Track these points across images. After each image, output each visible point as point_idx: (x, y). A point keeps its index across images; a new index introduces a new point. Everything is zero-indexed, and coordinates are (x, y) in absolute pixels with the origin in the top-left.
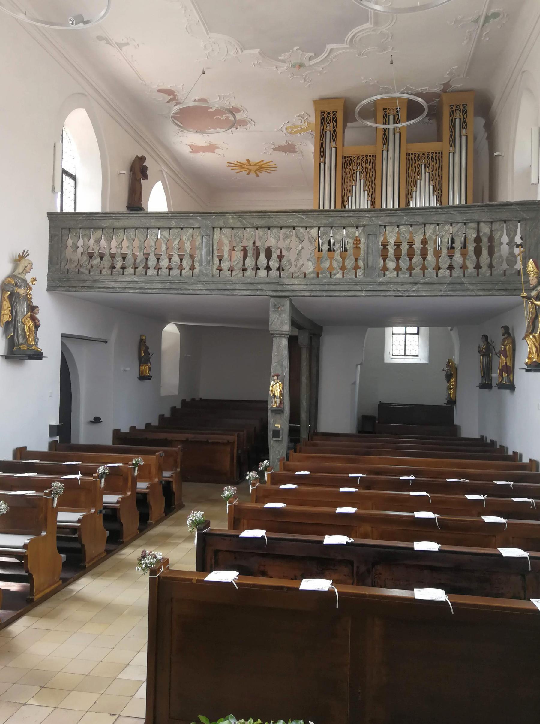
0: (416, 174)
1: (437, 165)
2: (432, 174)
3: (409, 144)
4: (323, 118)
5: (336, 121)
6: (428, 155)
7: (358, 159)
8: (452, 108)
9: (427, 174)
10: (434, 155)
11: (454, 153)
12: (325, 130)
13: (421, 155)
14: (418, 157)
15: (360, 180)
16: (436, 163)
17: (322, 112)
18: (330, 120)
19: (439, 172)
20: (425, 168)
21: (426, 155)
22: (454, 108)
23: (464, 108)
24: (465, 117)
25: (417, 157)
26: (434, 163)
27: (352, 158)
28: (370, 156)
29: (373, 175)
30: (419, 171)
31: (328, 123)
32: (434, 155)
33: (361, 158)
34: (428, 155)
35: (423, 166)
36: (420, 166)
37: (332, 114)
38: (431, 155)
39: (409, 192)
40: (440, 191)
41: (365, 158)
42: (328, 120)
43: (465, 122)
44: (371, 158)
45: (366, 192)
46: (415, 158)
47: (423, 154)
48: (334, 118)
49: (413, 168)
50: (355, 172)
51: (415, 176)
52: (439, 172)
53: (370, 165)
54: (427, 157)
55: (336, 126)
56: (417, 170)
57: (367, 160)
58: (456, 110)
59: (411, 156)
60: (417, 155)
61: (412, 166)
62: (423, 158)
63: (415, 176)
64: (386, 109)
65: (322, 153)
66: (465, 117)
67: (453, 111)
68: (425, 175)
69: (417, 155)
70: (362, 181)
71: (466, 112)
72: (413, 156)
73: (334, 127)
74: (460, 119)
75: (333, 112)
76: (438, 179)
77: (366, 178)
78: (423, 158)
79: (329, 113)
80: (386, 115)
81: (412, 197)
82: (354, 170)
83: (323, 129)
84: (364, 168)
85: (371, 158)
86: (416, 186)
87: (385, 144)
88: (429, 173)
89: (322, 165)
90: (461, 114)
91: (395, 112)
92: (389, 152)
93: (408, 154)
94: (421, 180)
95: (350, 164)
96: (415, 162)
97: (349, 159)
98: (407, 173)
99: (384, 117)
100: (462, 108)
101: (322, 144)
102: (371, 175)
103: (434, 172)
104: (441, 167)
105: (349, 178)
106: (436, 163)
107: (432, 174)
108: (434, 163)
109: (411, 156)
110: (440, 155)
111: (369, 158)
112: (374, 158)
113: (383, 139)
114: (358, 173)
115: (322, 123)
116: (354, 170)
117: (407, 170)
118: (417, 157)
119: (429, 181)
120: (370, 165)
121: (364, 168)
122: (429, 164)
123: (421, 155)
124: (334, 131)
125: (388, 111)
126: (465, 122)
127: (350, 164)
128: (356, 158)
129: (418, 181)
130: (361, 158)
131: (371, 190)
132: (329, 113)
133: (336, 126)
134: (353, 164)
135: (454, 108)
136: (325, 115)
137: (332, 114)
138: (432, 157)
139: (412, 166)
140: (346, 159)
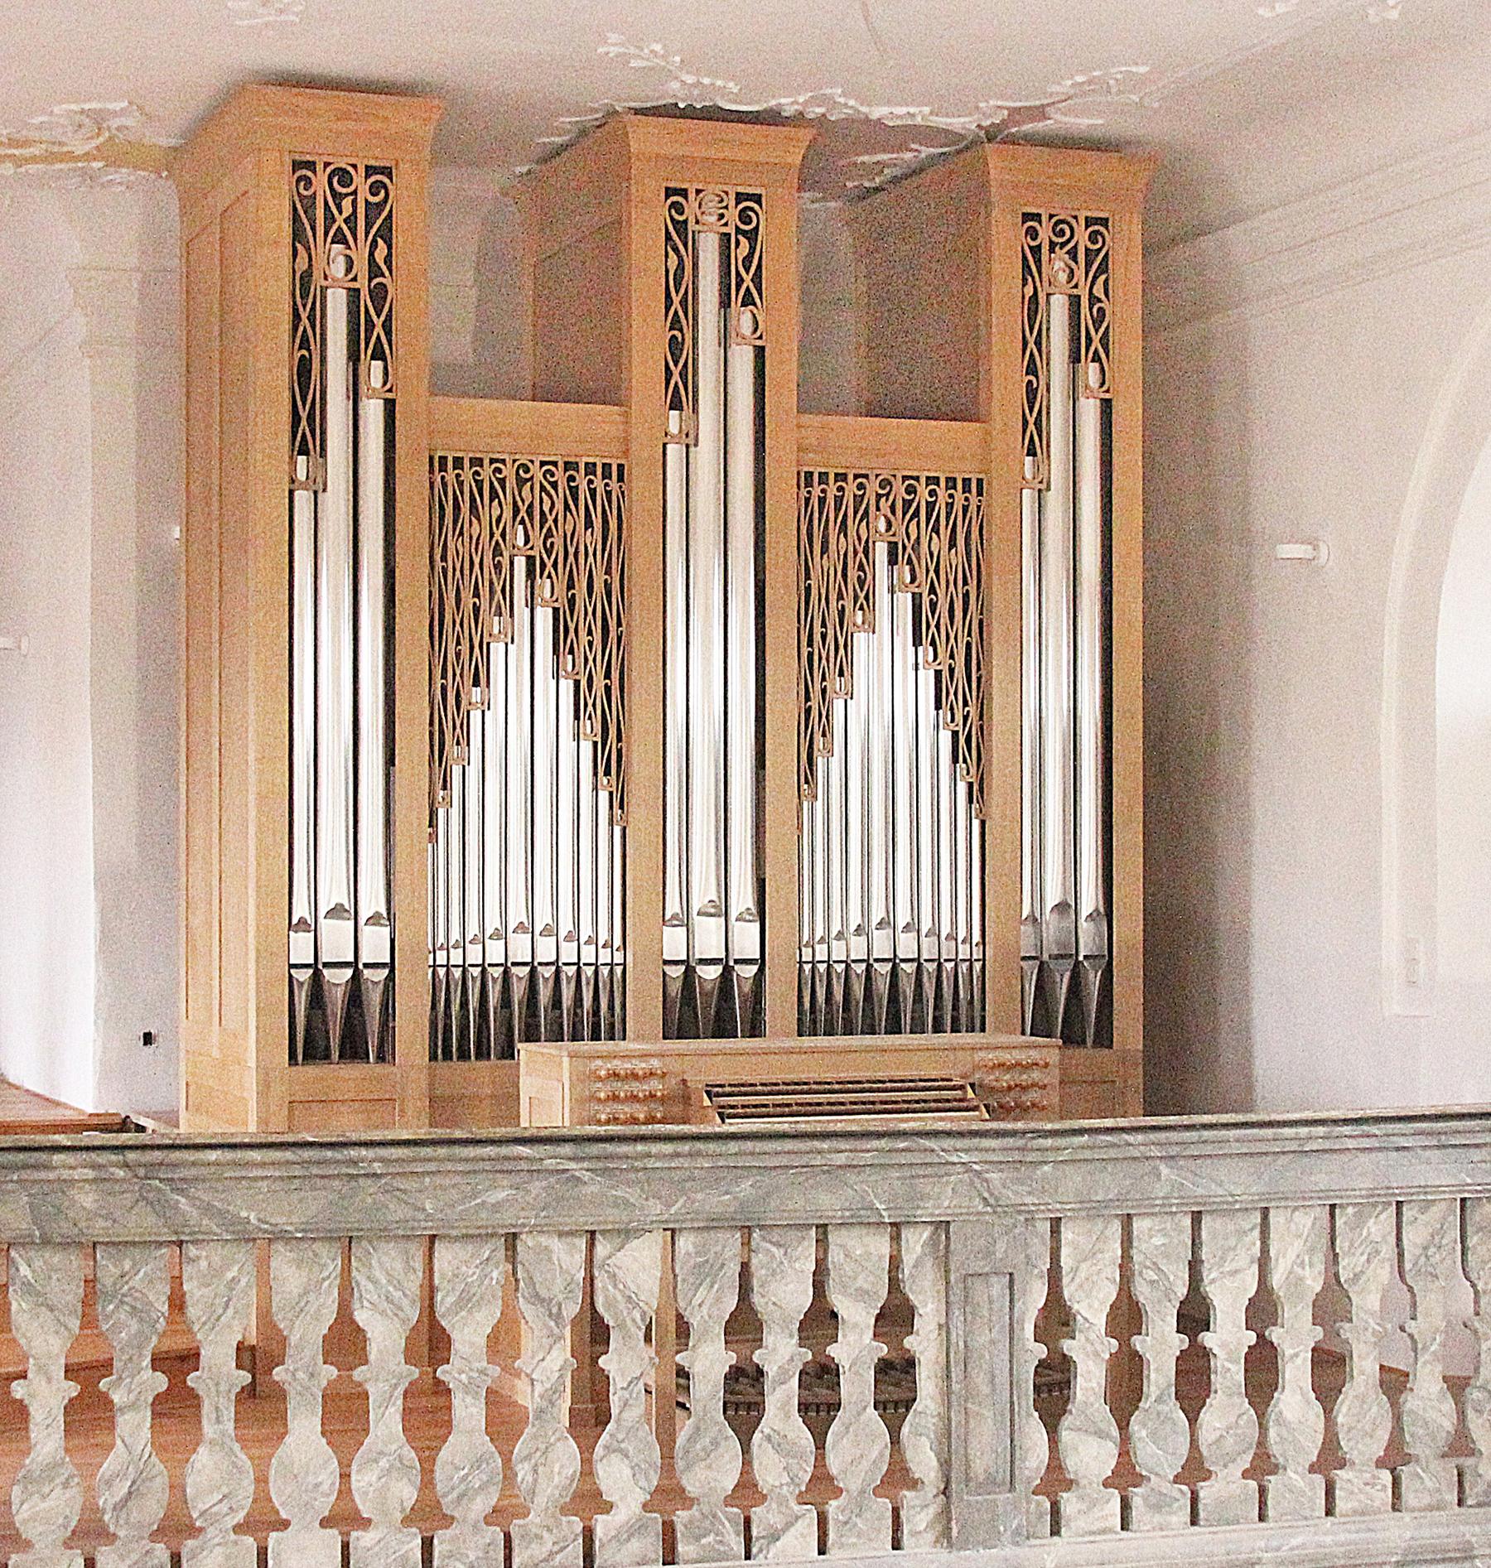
0: (848, 603)
1: (957, 558)
2: (933, 606)
4: (309, 204)
5: (386, 233)
6: (911, 490)
7: (521, 482)
8: (1033, 233)
10: (942, 493)
12: (318, 279)
13: (873, 487)
14: (858, 500)
16: (952, 544)
17: (296, 165)
18: (351, 220)
21: (899, 489)
22: (1045, 233)
23: (1093, 238)
24: (1098, 291)
25: (849, 499)
26: (940, 544)
27: (486, 472)
28: (590, 469)
31: (340, 238)
32: (942, 493)
34: (911, 490)
35: (881, 551)
37: (361, 183)
39: (814, 704)
40: (972, 710)
41: (560, 476)
42: (340, 221)
43: (1097, 323)
44: (599, 484)
46: (839, 501)
47: (885, 483)
48: (373, 210)
49: (832, 562)
52: (966, 595)
53: (589, 524)
54: (907, 504)
55: (388, 260)
56: (853, 574)
57: (574, 492)
58: (1052, 245)
59: (816, 491)
60: (851, 488)
61: (824, 550)
64: (684, 193)
66: (1098, 291)
67: (1036, 251)
70: (544, 617)
71: (1103, 268)
72: (832, 491)
73: (374, 271)
74: (1075, 301)
75: (370, 170)
77: (572, 601)
79: (344, 176)
80: (680, 227)
82: (497, 551)
83: (307, 276)
89: (302, 498)
90: (1080, 272)
91: (732, 215)
97: (467, 475)
99: (668, 237)
100: (1082, 237)
102: (598, 586)
103: (941, 592)
104: (976, 572)
105: (468, 600)
106: (952, 544)
107: (933, 606)
109: (816, 491)
110: (974, 500)
111: (582, 483)
115: (297, 235)
116: (497, 551)
118: (849, 499)
120: (589, 524)
123: (873, 487)
124: (379, 295)
125: (691, 208)
126: (1097, 323)
128: (508, 472)
132: (344, 176)
133: (388, 260)
135: (1045, 233)
136: (320, 182)
137: (361, 183)
138: (931, 506)
139: (824, 550)
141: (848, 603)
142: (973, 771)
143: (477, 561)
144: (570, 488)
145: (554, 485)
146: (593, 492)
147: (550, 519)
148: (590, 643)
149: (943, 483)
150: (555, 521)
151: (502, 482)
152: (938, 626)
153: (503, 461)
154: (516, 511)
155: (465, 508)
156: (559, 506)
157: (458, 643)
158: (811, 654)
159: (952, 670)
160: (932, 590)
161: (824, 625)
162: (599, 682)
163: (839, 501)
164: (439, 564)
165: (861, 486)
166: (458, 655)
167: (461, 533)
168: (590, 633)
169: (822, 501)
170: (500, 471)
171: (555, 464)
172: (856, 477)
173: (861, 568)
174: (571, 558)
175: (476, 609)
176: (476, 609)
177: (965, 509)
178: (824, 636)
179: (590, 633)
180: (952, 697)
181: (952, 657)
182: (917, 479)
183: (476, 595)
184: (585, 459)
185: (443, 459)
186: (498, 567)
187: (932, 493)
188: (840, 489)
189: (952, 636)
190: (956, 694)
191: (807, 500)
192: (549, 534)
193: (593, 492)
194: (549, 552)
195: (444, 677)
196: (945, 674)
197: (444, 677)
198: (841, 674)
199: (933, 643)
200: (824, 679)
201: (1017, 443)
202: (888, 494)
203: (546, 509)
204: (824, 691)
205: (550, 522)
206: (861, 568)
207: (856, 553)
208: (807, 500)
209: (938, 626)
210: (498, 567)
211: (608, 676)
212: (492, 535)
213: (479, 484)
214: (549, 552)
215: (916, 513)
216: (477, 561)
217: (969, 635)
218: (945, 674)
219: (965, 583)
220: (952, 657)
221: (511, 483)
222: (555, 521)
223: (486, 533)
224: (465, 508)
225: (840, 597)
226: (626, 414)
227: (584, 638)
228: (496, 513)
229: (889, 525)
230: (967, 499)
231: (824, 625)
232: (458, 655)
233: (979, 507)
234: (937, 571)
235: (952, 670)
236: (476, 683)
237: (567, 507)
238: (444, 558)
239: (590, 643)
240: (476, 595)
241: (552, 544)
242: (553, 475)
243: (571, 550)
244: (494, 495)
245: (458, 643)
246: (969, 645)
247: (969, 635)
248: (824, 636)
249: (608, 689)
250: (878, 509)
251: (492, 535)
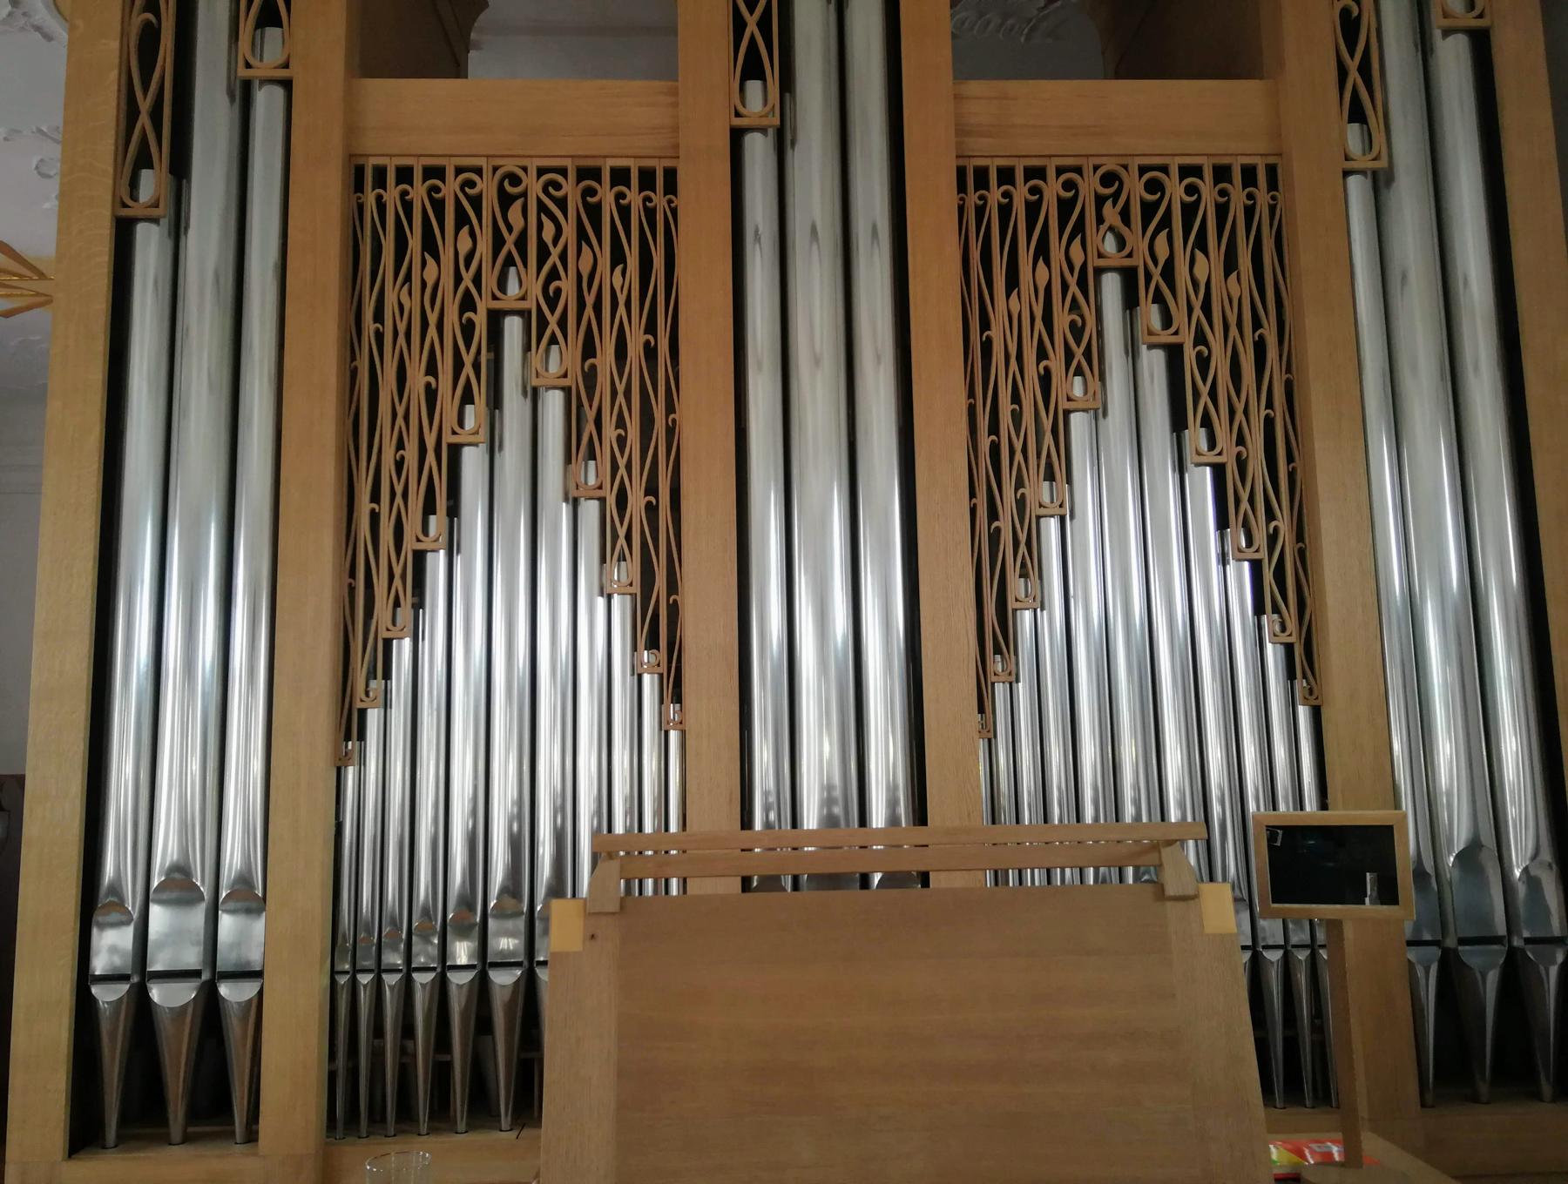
0: (1056, 363)
1: (1241, 286)
2: (1203, 363)
3: (975, 87)
6: (1154, 186)
7: (505, 200)
9: (1154, 363)
11: (1380, 182)
13: (1089, 186)
14: (1065, 207)
15: (534, 396)
16: (1230, 265)
19: (1260, 348)
20: (1130, 302)
21: (1135, 188)
26: (1208, 267)
27: (450, 188)
28: (620, 176)
29: (650, 353)
30: (1077, 331)
33: (534, 187)
34: (1154, 186)
35: (1111, 286)
36: (1087, 280)
38: (1176, 191)
39: (1005, 524)
44: (634, 198)
45: (590, 510)
46: (1033, 210)
47: (1109, 179)
49: (1025, 303)
50: (480, 319)
51: (1046, 380)
52: (1260, 348)
53: (618, 258)
54: (1148, 210)
56: (1062, 319)
57: (594, 212)
59: (995, 195)
60: (1053, 189)
61: (1012, 282)
62: (1111, 213)
63: (1046, 380)
65: (153, 128)
68: (1133, 382)
69: (1053, 189)
70: (553, 403)
72: (1021, 194)
76: (1258, 417)
77: (590, 377)
78: (1111, 213)
81: (1032, 566)
82: (468, 304)
84: (567, 285)
85: (634, 198)
86: (1058, 469)
87: (752, 69)
88: (1174, 354)
89: (149, 244)
92: (796, 159)
93: (971, 178)
94: (1099, 413)
95: (430, 246)
96: (1042, 252)
97: (418, 192)
98: (978, 356)
101: (149, 37)
104: (1274, 306)
105: (417, 380)
107: (1203, 363)
108: (1208, 267)
109: (995, 195)
111: (606, 196)
112: (659, 200)
113: (739, 25)
114: (513, 328)
116: (468, 304)
117: (976, 317)
119: (1178, 423)
120: (618, 258)
121: (567, 285)
122: (1169, 273)
123: (1089, 186)
127: (430, 246)
128: (487, 188)
129: (1079, 423)
130: (534, 187)
131: (637, 501)
134: (454, 243)
138: (1189, 211)
139: (1012, 282)
140: (392, 195)
141: (1056, 363)
142: (1292, 625)
143: (433, 318)
144: (585, 203)
145: (562, 203)
146: (624, 212)
147: (555, 252)
148: (622, 441)
149: (1208, 174)
150: (563, 257)
151: (476, 202)
152: (1213, 394)
153: (479, 171)
154: (498, 242)
155: (415, 242)
156: (569, 231)
157: (400, 446)
158: (995, 449)
159: (1242, 464)
160: (1200, 339)
161: (1016, 398)
162: (637, 501)
163: (1033, 210)
164: (369, 326)
165: (1069, 185)
166: (399, 464)
167: (408, 278)
168: (621, 423)
169: (1005, 211)
170: (472, 184)
171: (563, 172)
172: (1060, 171)
173: (1075, 307)
174: (589, 311)
175: (431, 394)
176: (431, 394)
177: (1249, 212)
178: (1017, 417)
179: (621, 423)
180: (1245, 505)
181: (1241, 441)
182: (1164, 169)
183: (432, 369)
184: (611, 163)
185: (380, 173)
186: (468, 329)
187: (1191, 189)
188: (1034, 190)
189: (1240, 408)
190: (1251, 500)
191: (980, 211)
192: (554, 275)
193: (624, 212)
194: (552, 302)
195: (375, 498)
196: (1231, 472)
197: (375, 498)
198: (1050, 476)
199: (1206, 422)
200: (1020, 484)
201: (1331, 106)
202: (1116, 197)
203: (548, 234)
204: (1021, 503)
205: (554, 258)
206: (1075, 307)
207: (1065, 287)
208: (980, 211)
209: (1213, 394)
210: (468, 329)
211: (651, 489)
212: (458, 279)
213: (439, 206)
214: (552, 302)
215: (1166, 222)
216: (433, 318)
217: (1270, 405)
218: (1231, 472)
219: (1257, 324)
220: (1241, 441)
221: (490, 202)
222: (563, 257)
223: (448, 281)
224: (415, 242)
225: (1042, 354)
226: (674, 92)
227: (610, 432)
228: (465, 244)
229: (1121, 243)
230: (1250, 196)
231: (1016, 398)
232: (399, 464)
233: (1272, 209)
234: (1207, 308)
235: (1242, 464)
236: (429, 508)
237: (582, 235)
238: (379, 316)
239: (622, 441)
240: (432, 369)
241: (558, 291)
242: (558, 187)
243: (590, 300)
244: (462, 220)
245: (400, 446)
246: (1269, 423)
247: (1270, 405)
248: (1017, 417)
249: (652, 510)
250: (1100, 220)
251: (458, 279)
